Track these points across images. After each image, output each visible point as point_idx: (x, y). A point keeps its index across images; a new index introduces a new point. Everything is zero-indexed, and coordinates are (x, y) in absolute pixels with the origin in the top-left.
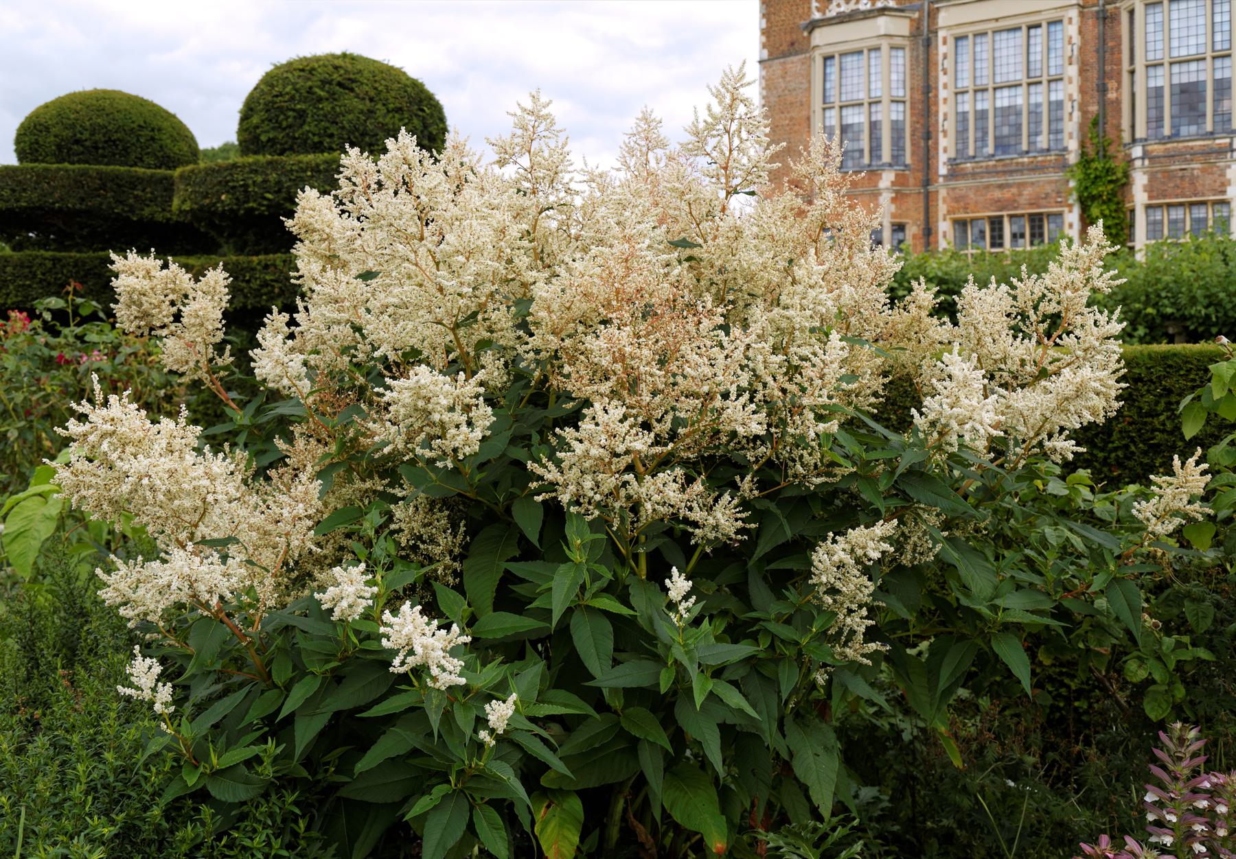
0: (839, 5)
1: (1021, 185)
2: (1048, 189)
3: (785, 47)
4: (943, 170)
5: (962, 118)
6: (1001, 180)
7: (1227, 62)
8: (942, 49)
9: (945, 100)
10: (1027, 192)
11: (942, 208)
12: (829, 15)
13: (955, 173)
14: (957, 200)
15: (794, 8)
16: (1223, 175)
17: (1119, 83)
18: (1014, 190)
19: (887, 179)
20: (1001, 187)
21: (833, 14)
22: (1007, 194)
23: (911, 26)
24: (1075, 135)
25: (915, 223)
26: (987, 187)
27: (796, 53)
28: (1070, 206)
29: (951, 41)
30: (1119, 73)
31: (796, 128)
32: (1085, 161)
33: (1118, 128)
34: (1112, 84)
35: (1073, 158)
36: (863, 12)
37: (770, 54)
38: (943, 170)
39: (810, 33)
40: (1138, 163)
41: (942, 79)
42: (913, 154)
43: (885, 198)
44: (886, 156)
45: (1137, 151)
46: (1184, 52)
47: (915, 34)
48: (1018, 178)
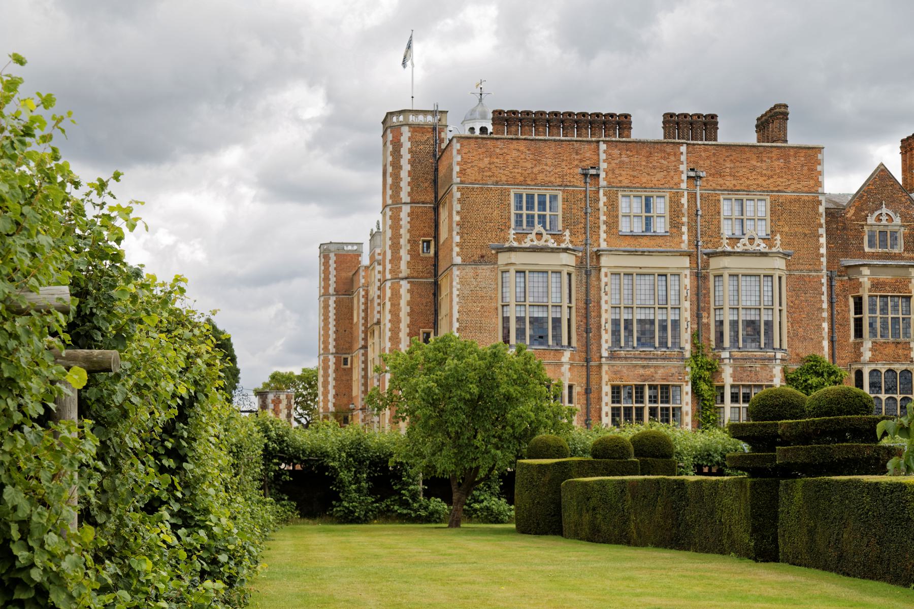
0: (532, 241)
1: (656, 367)
2: (673, 371)
3: (476, 258)
4: (605, 354)
5: (616, 323)
6: (645, 363)
7: (722, 312)
8: (604, 280)
9: (606, 311)
10: (661, 372)
11: (605, 378)
12: (524, 245)
13: (612, 356)
14: (615, 373)
15: (484, 233)
16: (771, 372)
17: (709, 314)
18: (652, 370)
19: (566, 356)
20: (644, 367)
21: (527, 245)
22: (648, 372)
23: (577, 261)
24: (689, 341)
25: (579, 385)
26: (635, 366)
27: (486, 263)
28: (687, 382)
29: (609, 274)
30: (709, 309)
31: (486, 314)
32: (695, 357)
33: (709, 340)
34: (705, 314)
35: (688, 355)
36: (552, 248)
37: (464, 260)
38: (605, 354)
39: (497, 253)
40: (727, 361)
41: (604, 298)
42: (578, 340)
43: (565, 368)
44: (565, 342)
45: (725, 355)
46: (749, 303)
47: (580, 265)
48: (654, 362)
